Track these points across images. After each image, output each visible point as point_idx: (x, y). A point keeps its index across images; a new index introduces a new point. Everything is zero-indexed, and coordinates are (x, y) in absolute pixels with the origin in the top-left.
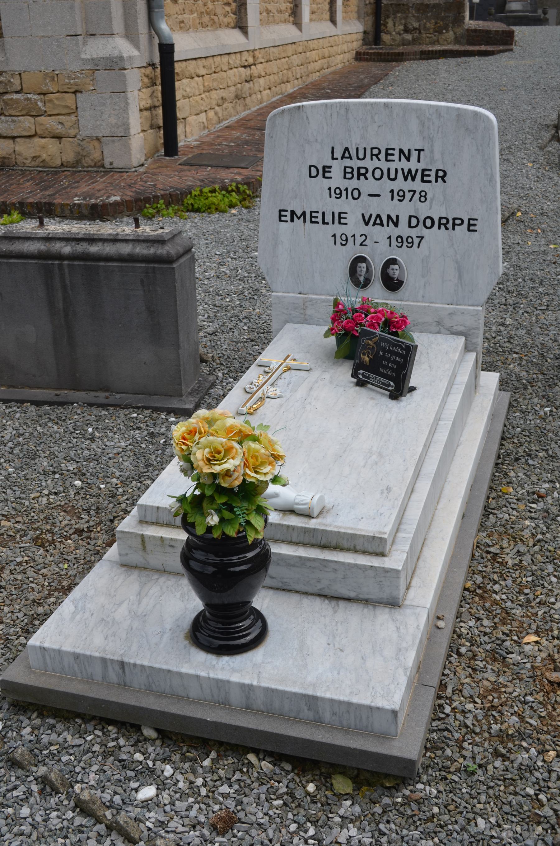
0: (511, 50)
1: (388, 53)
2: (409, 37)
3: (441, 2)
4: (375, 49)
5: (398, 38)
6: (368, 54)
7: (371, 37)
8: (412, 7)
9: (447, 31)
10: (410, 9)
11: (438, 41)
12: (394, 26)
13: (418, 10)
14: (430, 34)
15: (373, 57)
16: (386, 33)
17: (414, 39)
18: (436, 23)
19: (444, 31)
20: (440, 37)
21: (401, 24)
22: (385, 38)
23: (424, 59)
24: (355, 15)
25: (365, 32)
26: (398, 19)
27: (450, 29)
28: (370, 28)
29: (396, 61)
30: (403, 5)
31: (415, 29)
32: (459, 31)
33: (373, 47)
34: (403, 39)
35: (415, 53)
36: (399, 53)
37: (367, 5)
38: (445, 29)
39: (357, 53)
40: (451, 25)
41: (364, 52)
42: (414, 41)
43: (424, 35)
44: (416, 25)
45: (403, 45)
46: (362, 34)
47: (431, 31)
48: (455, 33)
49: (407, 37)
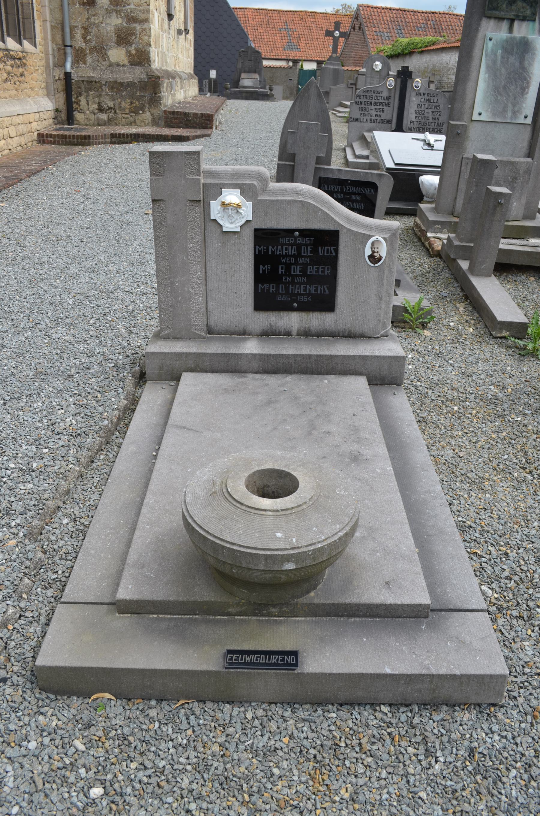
0: (209, 136)
1: (73, 136)
2: (104, 117)
3: (136, 81)
4: (67, 131)
5: (92, 117)
6: (51, 136)
7: (64, 116)
8: (105, 85)
9: (144, 112)
10: (103, 87)
11: (135, 122)
12: (88, 104)
13: (112, 88)
14: (126, 114)
15: (57, 139)
16: (79, 112)
17: (109, 120)
18: (132, 103)
19: (141, 112)
21: (95, 102)
22: (78, 116)
23: (115, 143)
24: (43, 92)
25: (57, 110)
26: (91, 97)
27: (147, 109)
28: (62, 106)
29: (83, 144)
30: (96, 82)
31: (110, 108)
32: (156, 112)
33: (66, 126)
34: (98, 119)
35: (104, 136)
36: (85, 136)
37: (56, 80)
39: (39, 135)
40: (148, 106)
41: (47, 134)
42: (109, 122)
43: (120, 116)
44: (111, 104)
45: (99, 125)
46: (53, 112)
47: (127, 111)
48: (152, 115)
49: (102, 117)
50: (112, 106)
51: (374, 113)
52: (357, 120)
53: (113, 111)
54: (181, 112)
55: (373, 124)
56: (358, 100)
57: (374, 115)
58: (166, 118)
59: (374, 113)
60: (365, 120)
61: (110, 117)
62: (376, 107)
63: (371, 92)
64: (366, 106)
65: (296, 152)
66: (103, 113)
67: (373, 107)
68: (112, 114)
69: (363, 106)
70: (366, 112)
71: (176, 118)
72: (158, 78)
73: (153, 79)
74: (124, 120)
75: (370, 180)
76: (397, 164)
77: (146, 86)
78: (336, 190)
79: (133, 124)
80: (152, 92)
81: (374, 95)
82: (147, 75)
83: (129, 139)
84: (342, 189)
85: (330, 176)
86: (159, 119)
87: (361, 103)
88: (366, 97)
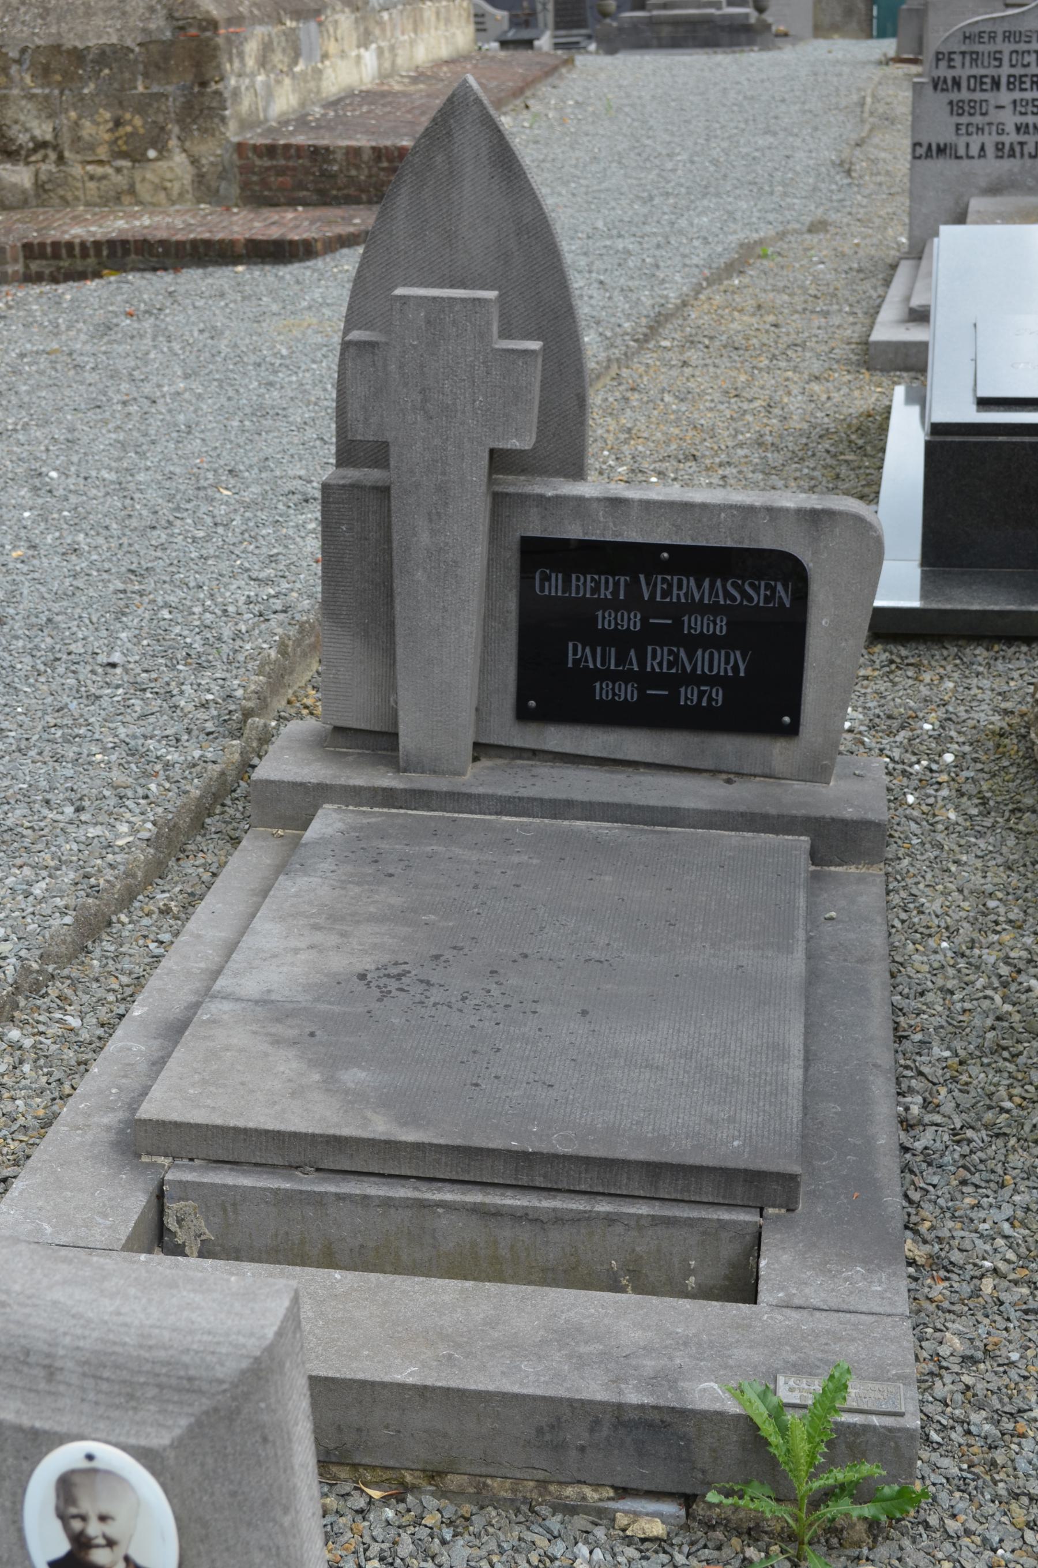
3: (129, 42)
8: (19, 62)
9: (164, 152)
10: (14, 69)
11: (132, 191)
13: (44, 73)
14: (100, 162)
17: (40, 187)
18: (118, 123)
19: (152, 154)
20: (138, 175)
27: (173, 143)
31: (41, 145)
32: (210, 151)
38: (153, 145)
40: (176, 130)
43: (77, 170)
44: (43, 130)
47: (103, 152)
48: (195, 161)
49: (15, 179)
50: (49, 137)
51: (1009, 119)
52: (941, 150)
53: (53, 156)
54: (299, 148)
55: (1007, 164)
56: (943, 71)
57: (1010, 128)
58: (246, 169)
59: (1009, 119)
60: (974, 150)
61: (43, 177)
62: (1017, 95)
63: (992, 37)
64: (978, 96)
65: (389, 436)
66: (15, 162)
67: (1005, 97)
68: (49, 167)
69: (965, 95)
70: (978, 119)
71: (281, 171)
72: (213, 24)
73: (193, 31)
74: (92, 185)
75: (767, 542)
76: (985, 403)
77: (166, 59)
78: (606, 593)
79: (126, 199)
80: (189, 77)
81: (1007, 48)
82: (170, 17)
83: (92, 261)
84: (633, 587)
85: (574, 531)
86: (221, 177)
87: (957, 83)
88: (975, 58)
